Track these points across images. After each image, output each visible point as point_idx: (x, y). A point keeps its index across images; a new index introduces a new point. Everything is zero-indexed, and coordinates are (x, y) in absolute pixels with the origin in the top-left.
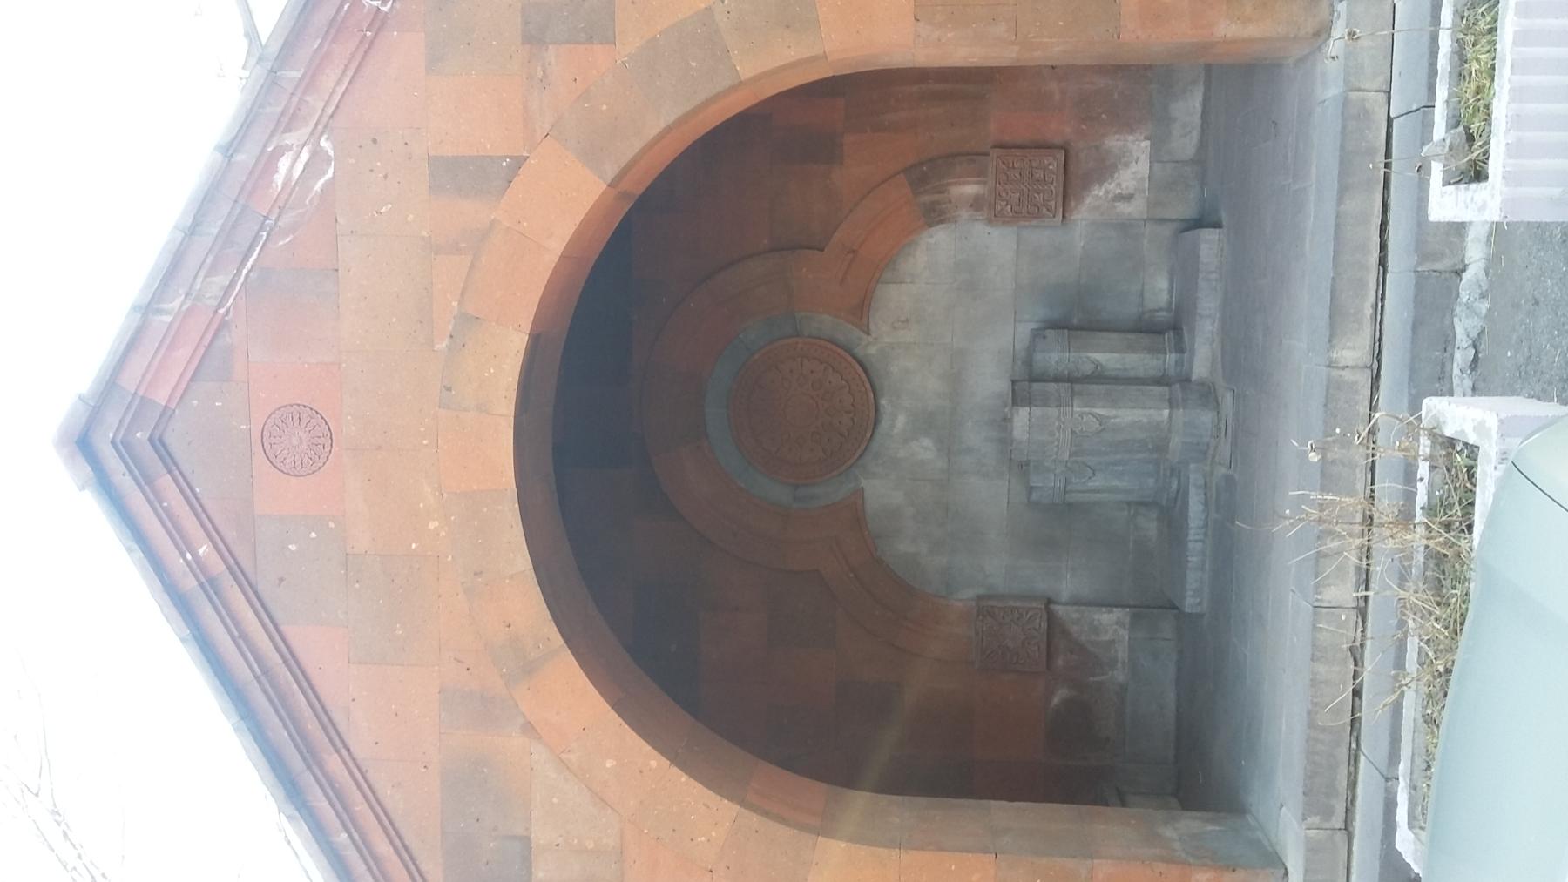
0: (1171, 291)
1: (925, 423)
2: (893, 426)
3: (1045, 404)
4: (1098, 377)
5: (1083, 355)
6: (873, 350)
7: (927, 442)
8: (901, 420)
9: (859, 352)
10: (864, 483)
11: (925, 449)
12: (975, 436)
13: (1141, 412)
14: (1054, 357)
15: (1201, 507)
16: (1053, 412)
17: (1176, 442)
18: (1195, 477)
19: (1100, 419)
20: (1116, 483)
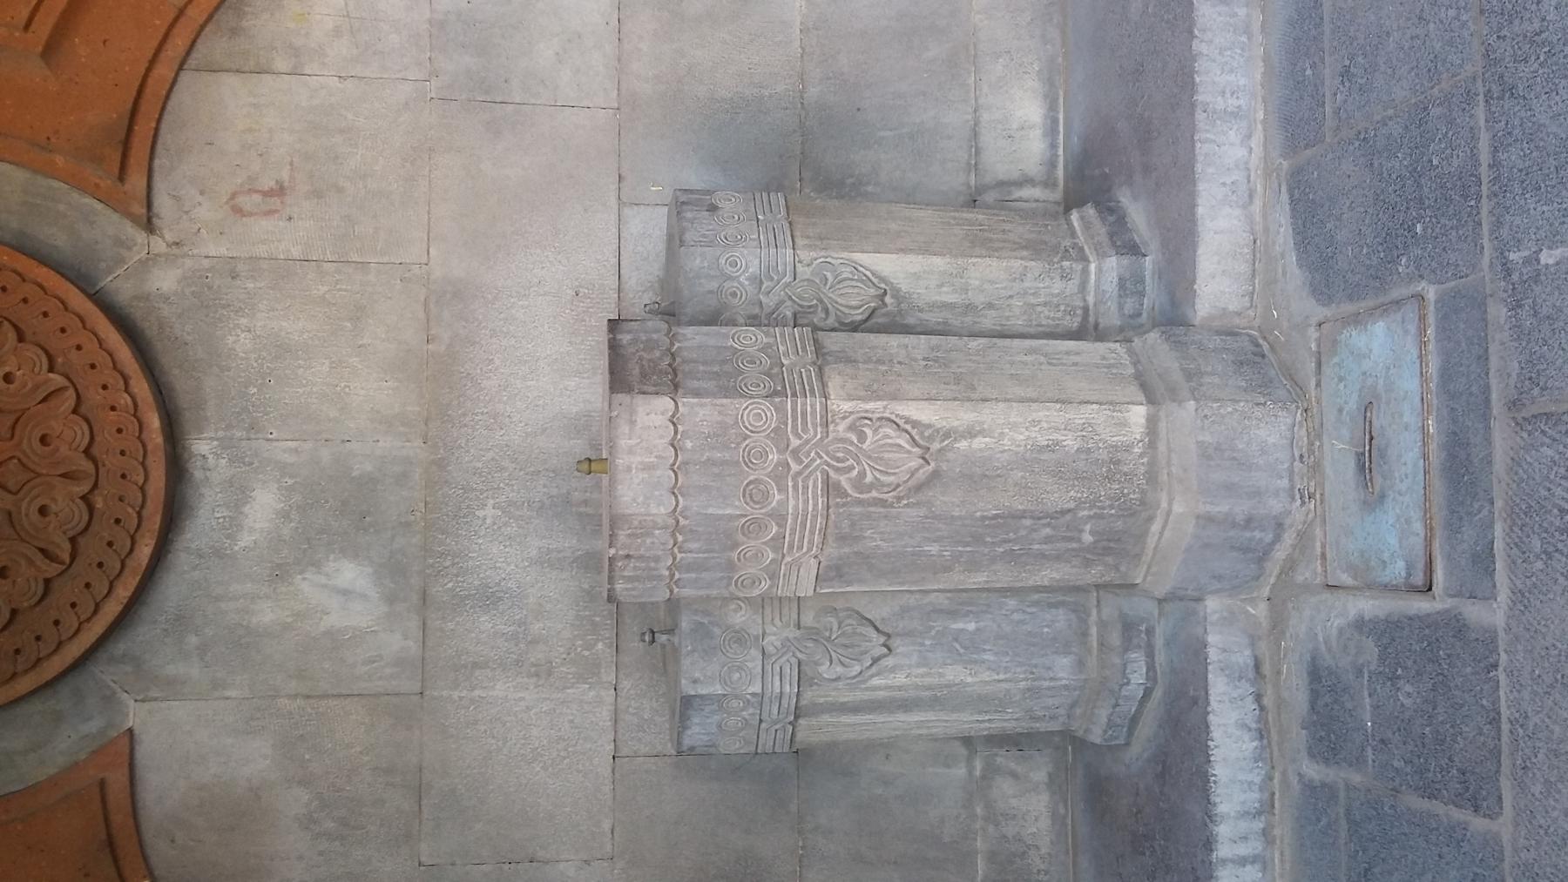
0: (1051, 131)
1: (344, 510)
2: (233, 526)
3: (728, 383)
4: (887, 317)
5: (838, 256)
6: (165, 280)
7: (350, 573)
8: (264, 507)
9: (121, 287)
10: (135, 714)
11: (343, 595)
12: (512, 555)
13: (1050, 415)
14: (750, 257)
15: (1249, 745)
16: (755, 413)
17: (1178, 513)
18: (1225, 648)
19: (922, 438)
20: (955, 674)
